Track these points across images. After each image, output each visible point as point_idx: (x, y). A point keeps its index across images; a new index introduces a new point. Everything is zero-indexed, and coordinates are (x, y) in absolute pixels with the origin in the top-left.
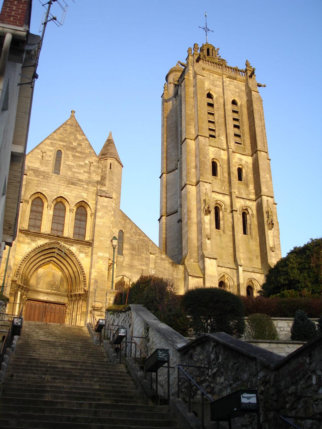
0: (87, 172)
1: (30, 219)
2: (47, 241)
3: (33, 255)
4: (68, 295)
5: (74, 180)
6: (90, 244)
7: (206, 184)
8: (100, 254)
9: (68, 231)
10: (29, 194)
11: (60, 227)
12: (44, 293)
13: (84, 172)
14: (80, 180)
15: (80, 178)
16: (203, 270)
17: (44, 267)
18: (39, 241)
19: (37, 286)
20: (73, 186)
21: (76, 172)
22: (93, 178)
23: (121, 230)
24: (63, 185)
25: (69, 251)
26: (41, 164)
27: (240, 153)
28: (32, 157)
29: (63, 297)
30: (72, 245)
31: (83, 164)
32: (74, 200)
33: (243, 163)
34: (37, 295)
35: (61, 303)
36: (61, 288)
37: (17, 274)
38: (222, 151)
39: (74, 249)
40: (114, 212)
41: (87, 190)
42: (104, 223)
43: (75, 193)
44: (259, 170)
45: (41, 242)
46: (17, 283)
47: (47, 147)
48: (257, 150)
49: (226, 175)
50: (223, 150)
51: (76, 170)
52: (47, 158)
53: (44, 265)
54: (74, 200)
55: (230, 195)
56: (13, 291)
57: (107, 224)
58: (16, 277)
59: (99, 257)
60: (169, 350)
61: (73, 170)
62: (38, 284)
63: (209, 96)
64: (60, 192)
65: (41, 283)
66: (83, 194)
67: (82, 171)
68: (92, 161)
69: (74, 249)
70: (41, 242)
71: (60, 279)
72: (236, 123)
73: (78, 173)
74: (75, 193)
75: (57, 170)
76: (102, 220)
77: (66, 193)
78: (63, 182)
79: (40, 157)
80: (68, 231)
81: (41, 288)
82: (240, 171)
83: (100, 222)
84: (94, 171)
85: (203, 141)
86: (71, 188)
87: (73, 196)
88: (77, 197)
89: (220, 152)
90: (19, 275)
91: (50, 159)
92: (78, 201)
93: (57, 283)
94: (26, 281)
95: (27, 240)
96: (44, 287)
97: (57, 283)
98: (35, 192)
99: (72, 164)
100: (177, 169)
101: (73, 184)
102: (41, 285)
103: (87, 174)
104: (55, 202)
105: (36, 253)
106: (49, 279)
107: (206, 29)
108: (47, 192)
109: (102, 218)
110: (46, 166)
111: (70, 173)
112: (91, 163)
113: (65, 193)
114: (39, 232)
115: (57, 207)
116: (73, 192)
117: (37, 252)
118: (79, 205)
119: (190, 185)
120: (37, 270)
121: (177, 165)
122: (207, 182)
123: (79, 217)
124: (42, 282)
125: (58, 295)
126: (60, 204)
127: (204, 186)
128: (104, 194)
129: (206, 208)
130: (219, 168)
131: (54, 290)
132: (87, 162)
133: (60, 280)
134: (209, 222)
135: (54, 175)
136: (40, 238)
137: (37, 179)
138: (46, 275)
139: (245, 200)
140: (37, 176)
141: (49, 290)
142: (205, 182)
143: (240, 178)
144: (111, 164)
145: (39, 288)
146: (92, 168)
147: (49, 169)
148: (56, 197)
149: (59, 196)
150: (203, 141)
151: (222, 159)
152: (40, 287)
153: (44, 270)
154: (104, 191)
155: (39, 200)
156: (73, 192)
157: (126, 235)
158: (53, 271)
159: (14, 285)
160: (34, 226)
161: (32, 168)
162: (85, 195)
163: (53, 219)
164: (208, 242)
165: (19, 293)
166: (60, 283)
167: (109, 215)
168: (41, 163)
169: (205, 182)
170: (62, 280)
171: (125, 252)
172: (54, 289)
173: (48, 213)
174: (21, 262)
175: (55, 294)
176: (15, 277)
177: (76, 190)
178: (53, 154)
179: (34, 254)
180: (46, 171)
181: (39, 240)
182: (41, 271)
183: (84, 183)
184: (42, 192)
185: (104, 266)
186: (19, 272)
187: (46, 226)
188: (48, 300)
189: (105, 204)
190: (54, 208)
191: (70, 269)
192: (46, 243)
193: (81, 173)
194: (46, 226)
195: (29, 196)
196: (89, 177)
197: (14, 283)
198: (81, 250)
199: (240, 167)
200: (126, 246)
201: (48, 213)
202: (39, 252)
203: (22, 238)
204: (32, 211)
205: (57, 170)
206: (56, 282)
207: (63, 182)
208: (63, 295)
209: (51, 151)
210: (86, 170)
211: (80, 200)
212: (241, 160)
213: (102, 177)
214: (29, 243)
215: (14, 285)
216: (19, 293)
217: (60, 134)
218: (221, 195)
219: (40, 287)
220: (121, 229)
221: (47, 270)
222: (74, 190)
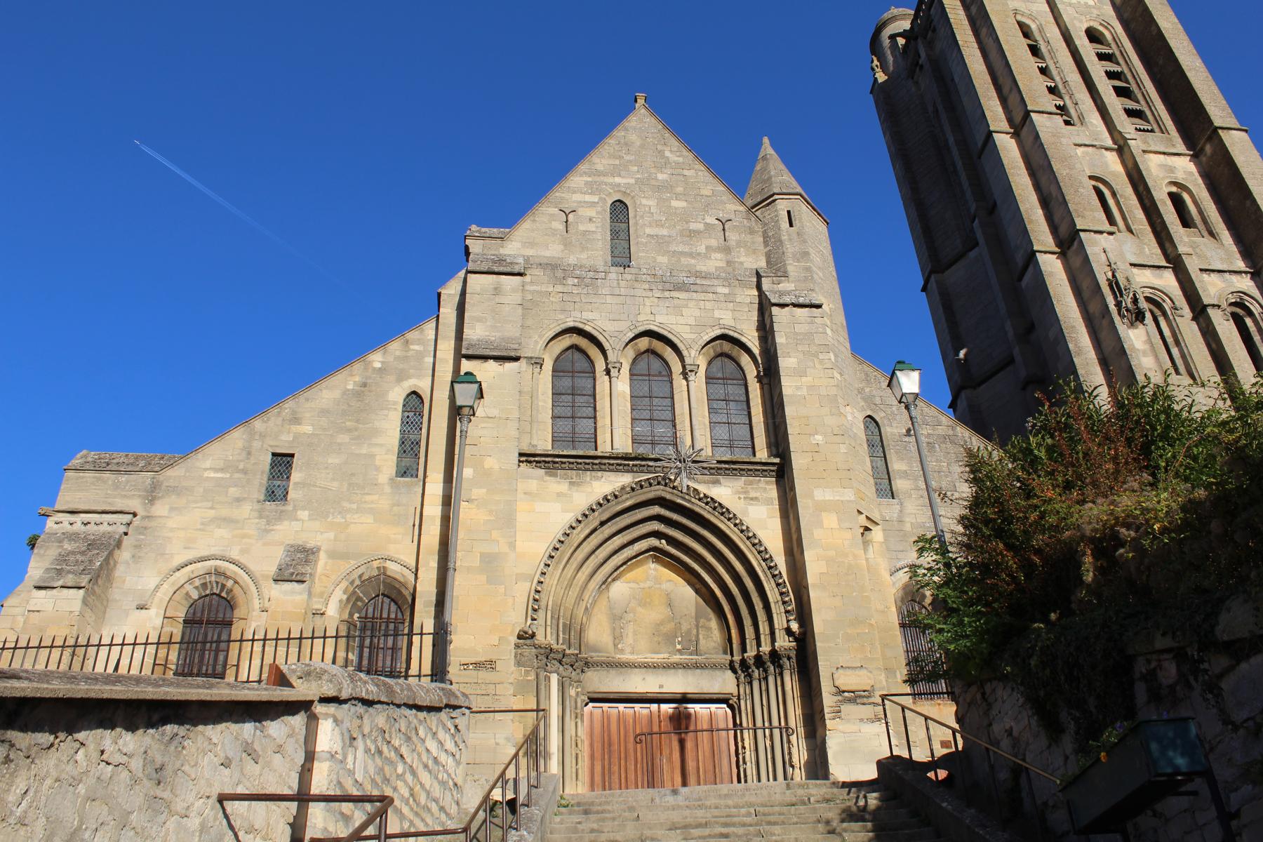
0: (718, 250)
1: (553, 417)
2: (626, 479)
3: (582, 536)
4: (732, 662)
5: (682, 277)
7: (1098, 236)
8: (821, 495)
10: (541, 336)
11: (662, 430)
12: (646, 666)
13: (707, 248)
14: (698, 275)
15: (702, 267)
17: (630, 575)
18: (596, 484)
20: (682, 295)
21: (682, 253)
22: (742, 263)
23: (869, 416)
24: (650, 294)
25: (707, 503)
26: (565, 245)
27: (1162, 150)
28: (533, 230)
29: (718, 673)
30: (717, 482)
31: (701, 226)
32: (693, 336)
35: (715, 697)
36: (702, 642)
37: (535, 610)
38: (1108, 154)
40: (836, 356)
41: (729, 299)
42: (811, 388)
44: (1243, 179)
46: (540, 638)
47: (577, 197)
48: (1217, 128)
50: (1107, 149)
52: (582, 228)
53: (630, 569)
54: (693, 336)
56: (527, 673)
57: (823, 392)
58: (534, 619)
59: (822, 507)
61: (673, 247)
62: (617, 638)
64: (641, 318)
65: (630, 635)
66: (717, 314)
67: (702, 249)
68: (727, 217)
72: (1118, 83)
73: (691, 255)
75: (622, 257)
76: (804, 379)
77: (663, 321)
78: (647, 286)
79: (561, 227)
81: (632, 653)
82: (1176, 200)
83: (798, 388)
84: (739, 244)
85: (1048, 124)
86: (676, 301)
87: (690, 323)
88: (700, 326)
89: (1102, 156)
90: (541, 614)
91: (591, 227)
92: (707, 338)
93: (685, 627)
94: (573, 630)
95: (556, 484)
97: (685, 627)
98: (559, 329)
99: (665, 232)
100: (977, 244)
102: (629, 640)
103: (719, 256)
104: (630, 353)
105: (592, 527)
106: (654, 614)
108: (599, 323)
110: (584, 249)
111: (663, 260)
113: (659, 319)
114: (592, 453)
115: (642, 366)
116: (685, 311)
117: (597, 523)
118: (712, 354)
119: (1045, 252)
120: (607, 588)
121: (972, 230)
122: (1101, 232)
123: (720, 391)
124: (630, 629)
127: (1095, 243)
128: (787, 300)
129: (1128, 301)
131: (679, 651)
132: (711, 220)
134: (1147, 347)
135: (613, 269)
136: (600, 474)
137: (559, 288)
138: (645, 600)
139: (1227, 275)
141: (662, 656)
142: (1096, 232)
143: (1186, 222)
144: (789, 212)
145: (622, 651)
146: (733, 237)
148: (631, 335)
149: (642, 329)
150: (1048, 124)
151: (1114, 174)
152: (628, 650)
153: (633, 585)
154: (789, 293)
155: (577, 355)
156: (685, 311)
157: (888, 429)
158: (664, 586)
159: (530, 652)
160: (573, 442)
161: (537, 261)
163: (632, 409)
165: (554, 678)
166: (697, 626)
167: (821, 362)
168: (567, 244)
169: (1096, 232)
171: (899, 484)
172: (679, 647)
173: (616, 392)
174: (542, 565)
175: (685, 666)
176: (529, 621)
177: (691, 304)
178: (598, 213)
179: (587, 531)
180: (584, 262)
181: (598, 479)
182: (619, 589)
183: (716, 282)
184: (581, 326)
185: (848, 535)
186: (543, 604)
187: (616, 433)
189: (800, 329)
190: (631, 375)
192: (623, 488)
193: (699, 254)
194: (616, 433)
195: (542, 343)
196: (729, 263)
197: (528, 642)
198: (753, 494)
199: (1174, 189)
201: (616, 392)
202: (603, 524)
203: (535, 482)
204: (556, 394)
205: (622, 257)
206: (683, 621)
207: (647, 286)
208: (714, 666)
209: (593, 204)
210: (714, 243)
211: (713, 334)
212: (1171, 170)
213: (768, 256)
214: (559, 495)
215: (530, 652)
216: (554, 678)
217: (612, 156)
218: (1148, 272)
219: (628, 650)
220: (869, 413)
221: (642, 585)
222: (686, 306)
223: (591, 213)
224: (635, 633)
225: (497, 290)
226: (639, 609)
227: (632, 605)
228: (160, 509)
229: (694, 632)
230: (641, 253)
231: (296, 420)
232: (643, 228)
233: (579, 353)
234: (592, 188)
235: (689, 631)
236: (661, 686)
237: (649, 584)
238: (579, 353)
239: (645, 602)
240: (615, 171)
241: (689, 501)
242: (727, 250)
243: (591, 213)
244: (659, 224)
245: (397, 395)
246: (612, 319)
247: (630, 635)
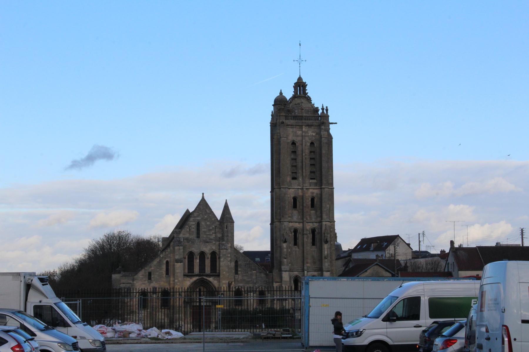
2: (197, 278)
5: (208, 240)
6: (219, 276)
8: (224, 282)
9: (208, 270)
16: (281, 277)
33: (315, 195)
39: (211, 279)
43: (209, 247)
45: (195, 279)
49: (301, 207)
51: (208, 233)
55: (303, 222)
60: (337, 259)
63: (294, 143)
69: (211, 279)
70: (195, 279)
74: (209, 247)
75: (198, 236)
79: (188, 230)
80: (208, 270)
87: (207, 249)
95: (188, 279)
99: (205, 230)
101: (207, 242)
107: (300, 61)
109: (223, 261)
112: (216, 227)
126: (202, 255)
130: (298, 202)
132: (213, 226)
140: (188, 242)
146: (217, 230)
147: (194, 236)
162: (214, 248)
164: (285, 260)
168: (190, 234)
171: (239, 273)
173: (197, 262)
187: (197, 270)
189: (224, 253)
194: (197, 270)
200: (239, 269)
201: (197, 262)
205: (198, 236)
210: (213, 232)
217: (198, 212)
223: (193, 226)
225: (179, 249)
228: (135, 282)
230: (202, 235)
231: (151, 267)
232: (203, 230)
233: (191, 255)
234: (194, 221)
238: (191, 255)
240: (198, 216)
242: (215, 233)
243: (193, 226)
244: (204, 228)
245: (165, 262)
246: (196, 250)
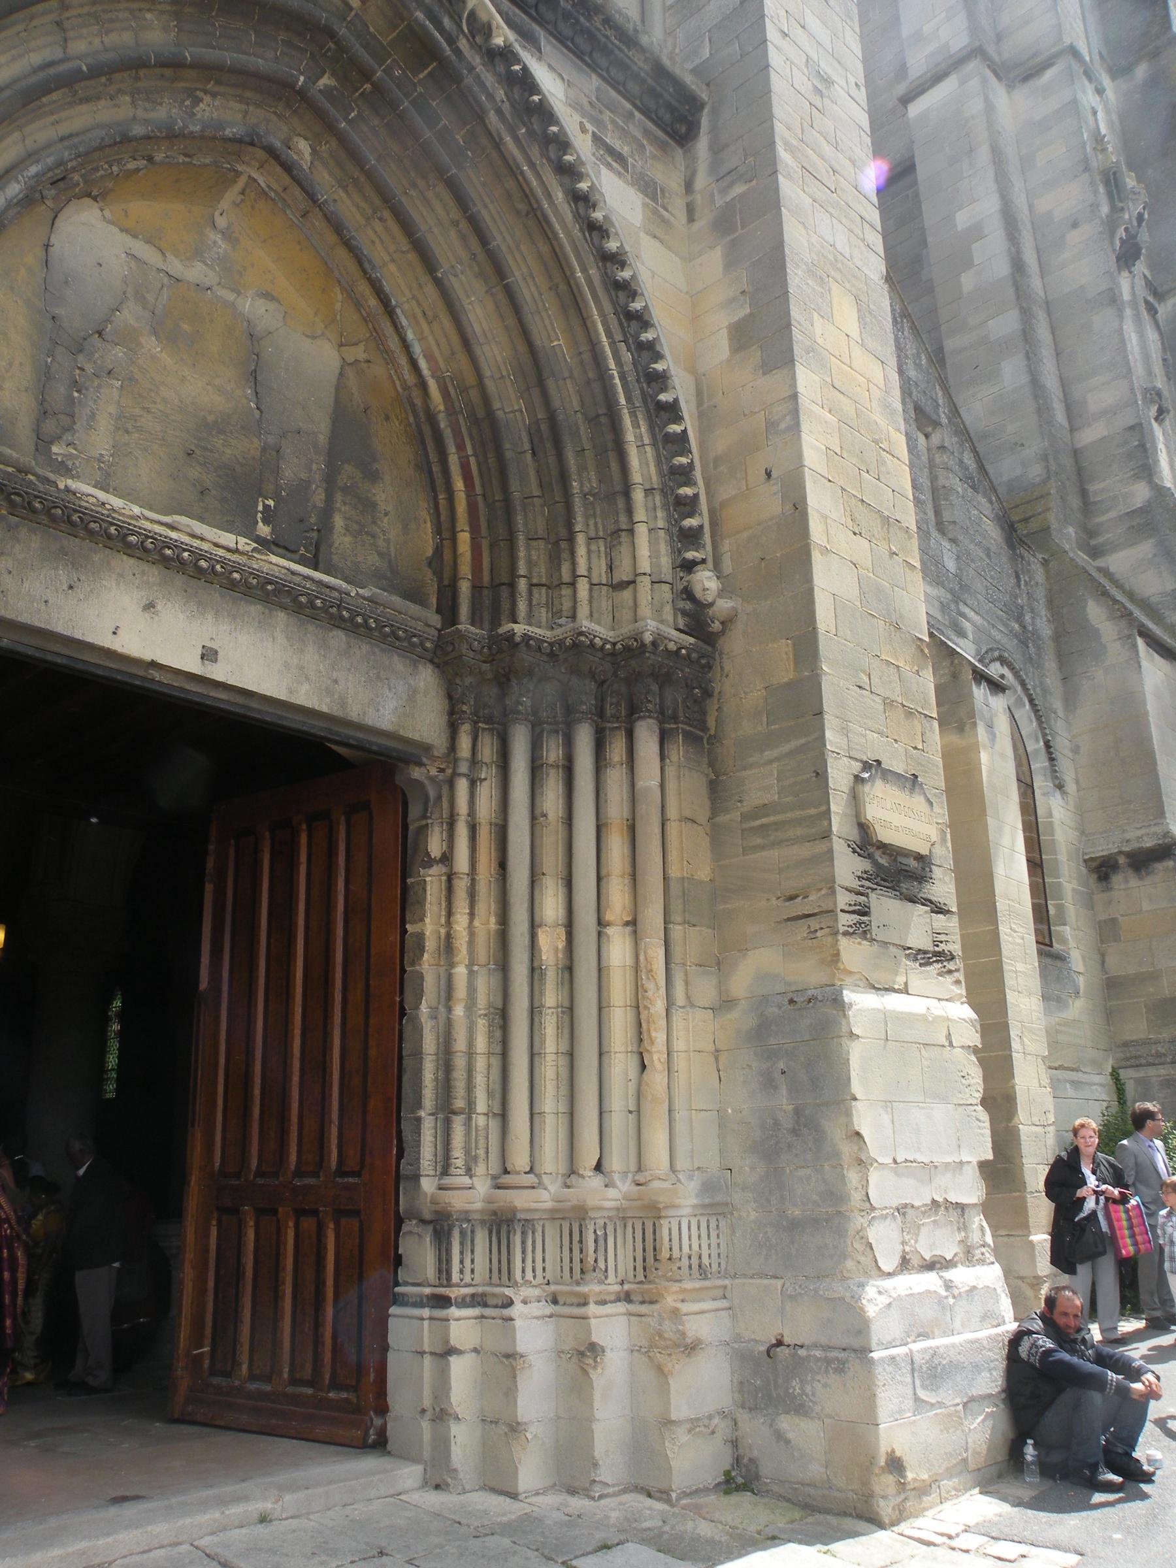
19: (43, 443)
29: (398, 663)
34: (63, 575)
65: (104, 423)
71: (321, 427)
93: (291, 470)
96: (145, 470)
102: (99, 439)
106: (198, 386)
124: (105, 403)
125: (337, 622)
133: (322, 439)
170: (348, 435)
182: (95, 241)
188: (218, 672)
191: (480, 313)
221: (176, 266)
224: (123, 423)
226: (150, 344)
227: (130, 315)
229: (319, 498)
235: (302, 489)
236: (208, 655)
237: (196, 272)
239: (166, 329)
241: (451, 41)
247: (104, 423)
